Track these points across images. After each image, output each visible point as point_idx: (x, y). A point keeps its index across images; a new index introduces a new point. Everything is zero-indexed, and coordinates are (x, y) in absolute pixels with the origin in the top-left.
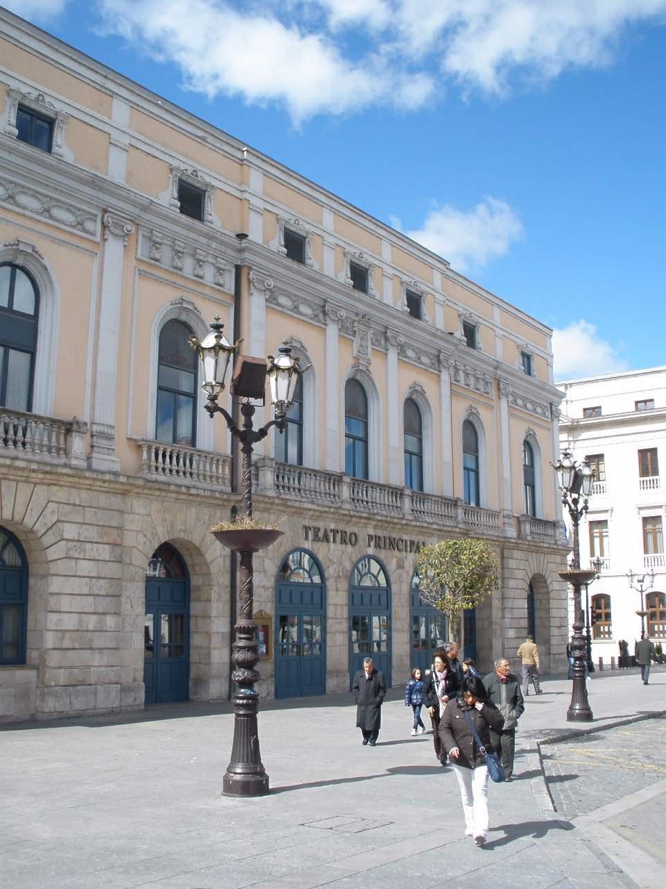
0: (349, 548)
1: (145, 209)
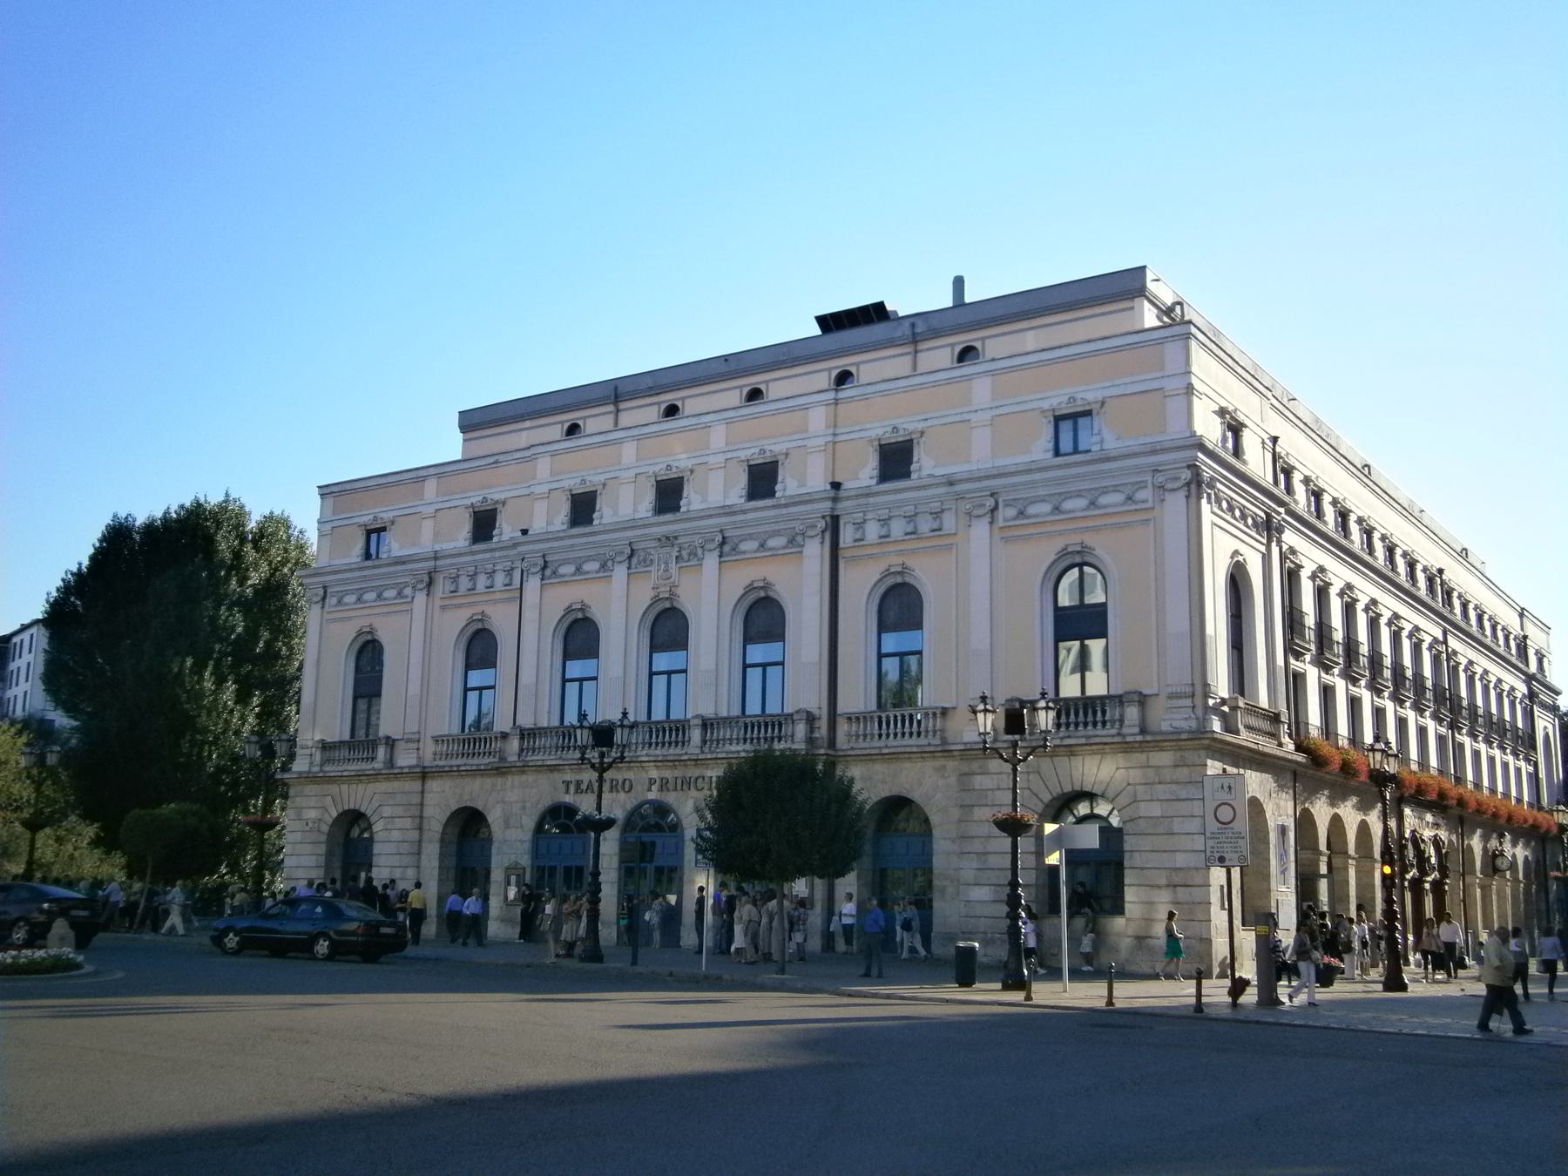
0: (622, 796)
1: (436, 558)
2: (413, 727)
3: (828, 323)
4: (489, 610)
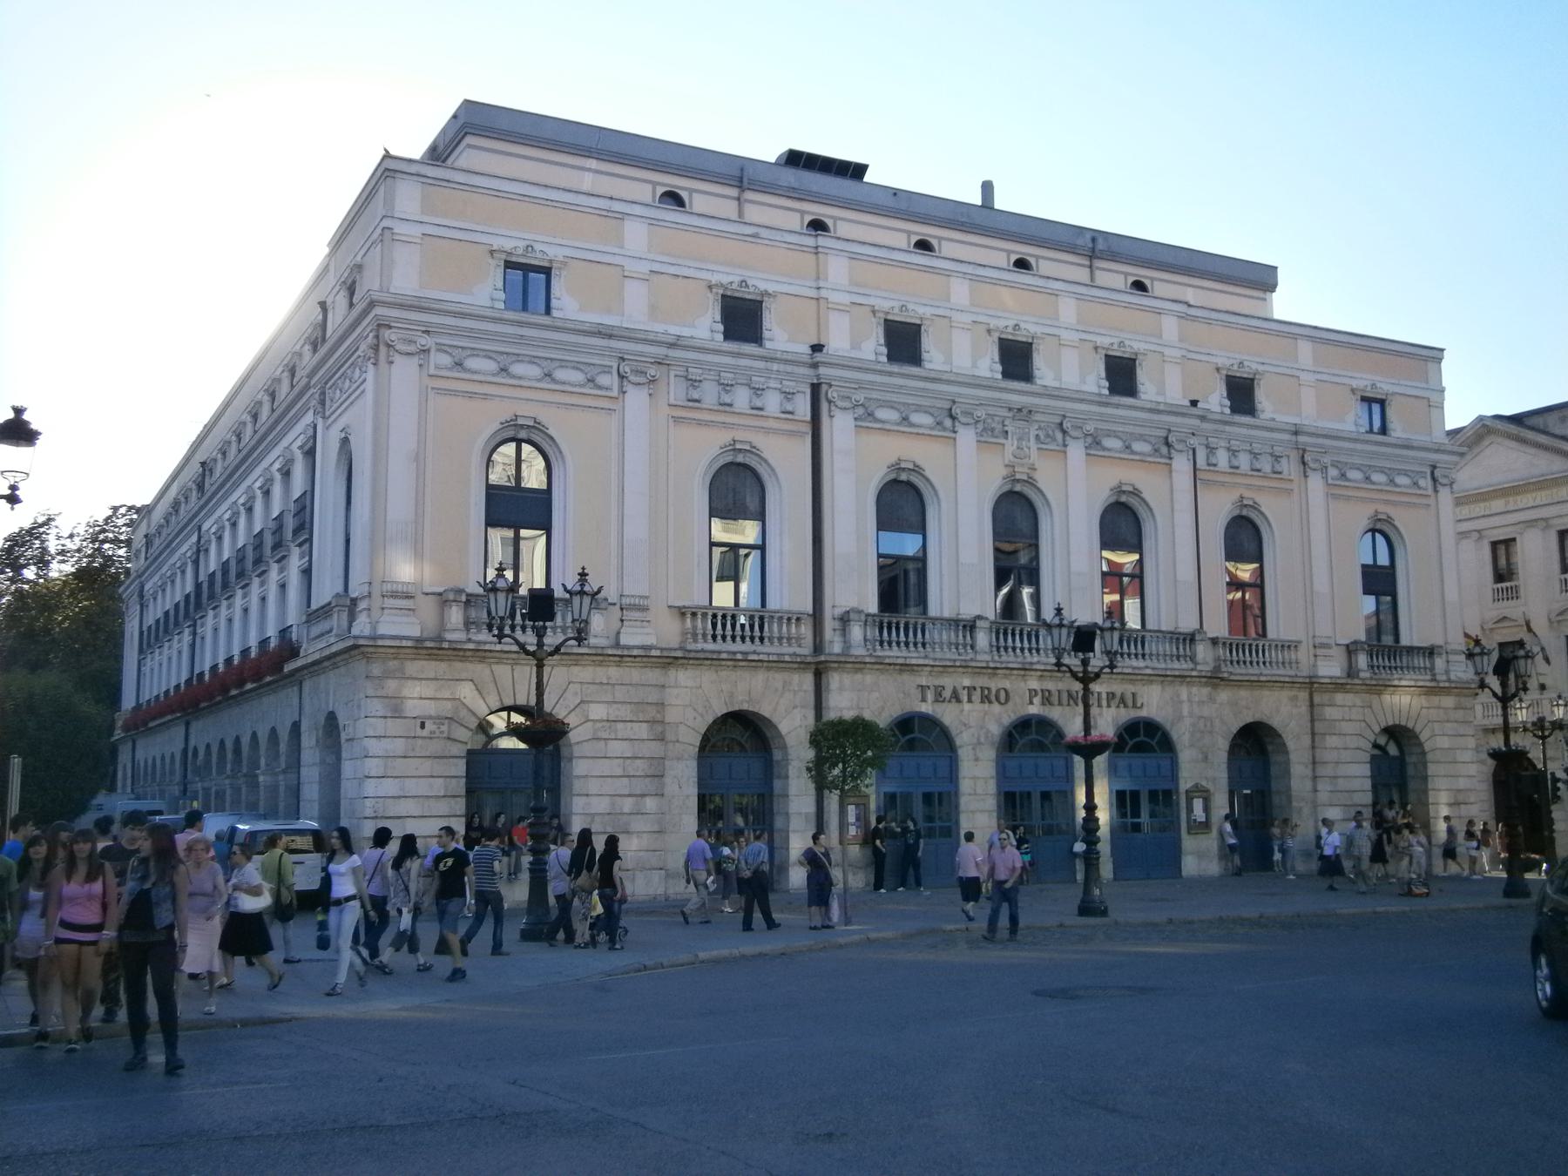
0: (996, 707)
1: (672, 346)
2: (635, 587)
3: (795, 159)
4: (760, 441)
